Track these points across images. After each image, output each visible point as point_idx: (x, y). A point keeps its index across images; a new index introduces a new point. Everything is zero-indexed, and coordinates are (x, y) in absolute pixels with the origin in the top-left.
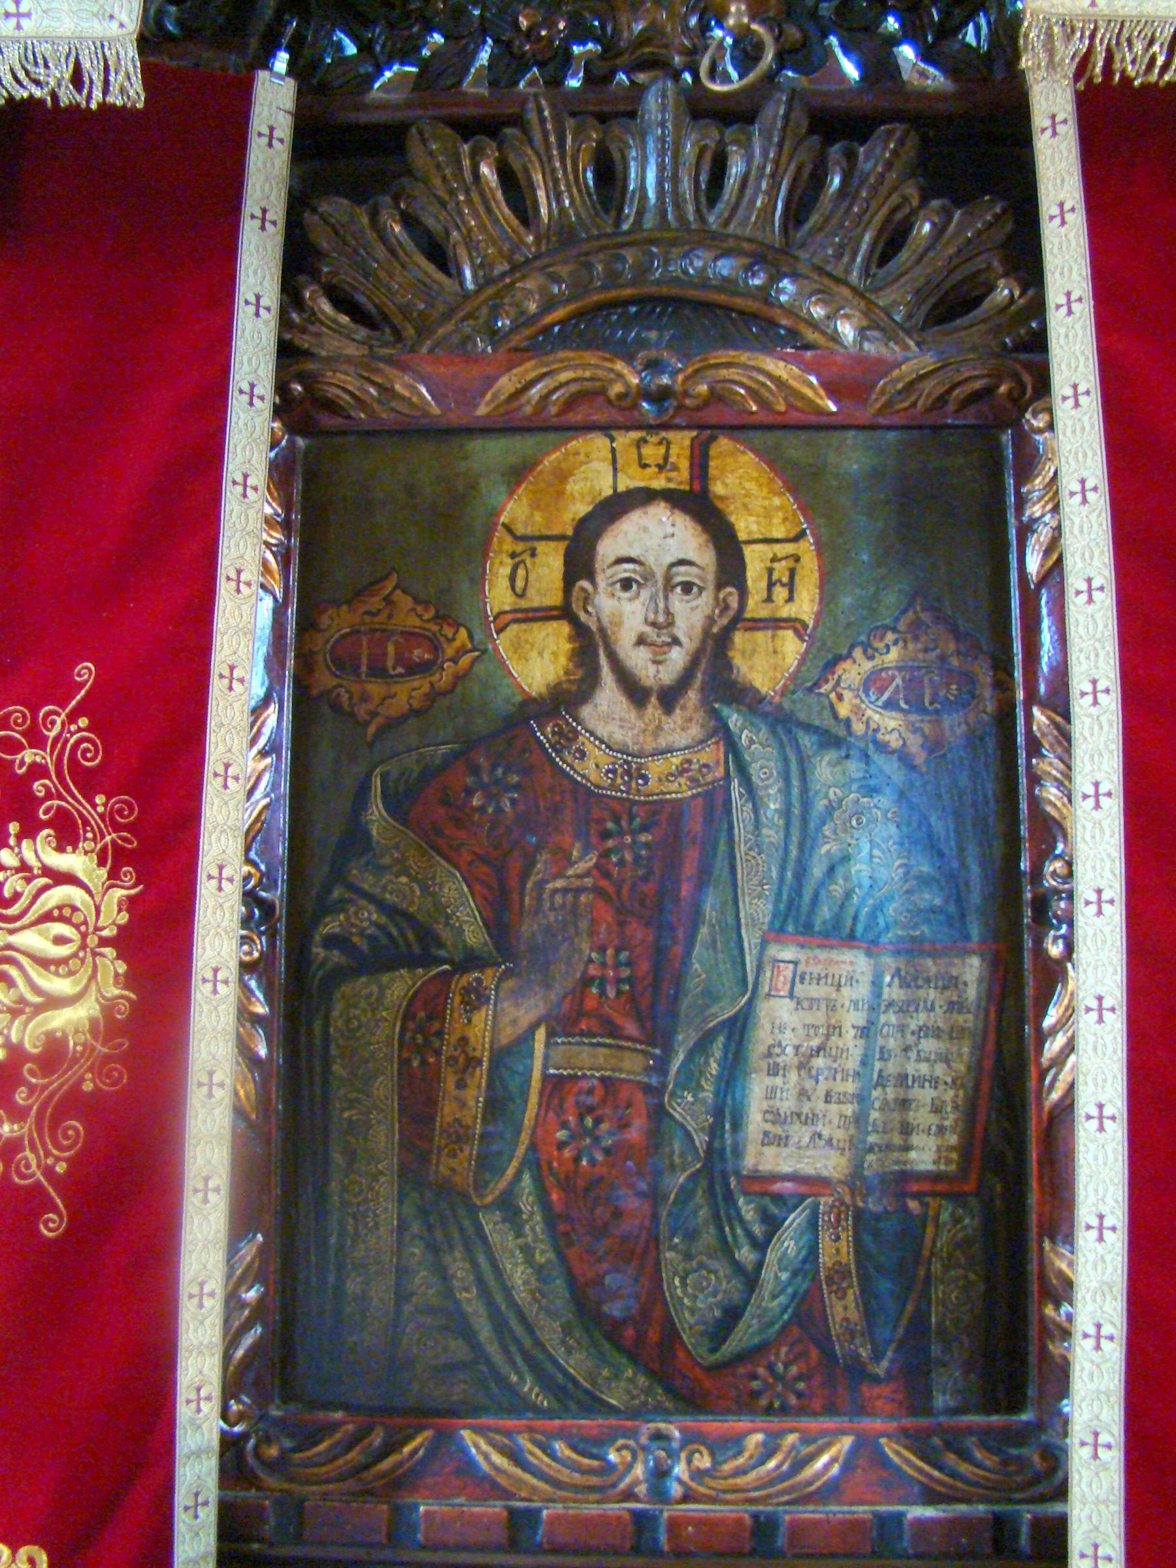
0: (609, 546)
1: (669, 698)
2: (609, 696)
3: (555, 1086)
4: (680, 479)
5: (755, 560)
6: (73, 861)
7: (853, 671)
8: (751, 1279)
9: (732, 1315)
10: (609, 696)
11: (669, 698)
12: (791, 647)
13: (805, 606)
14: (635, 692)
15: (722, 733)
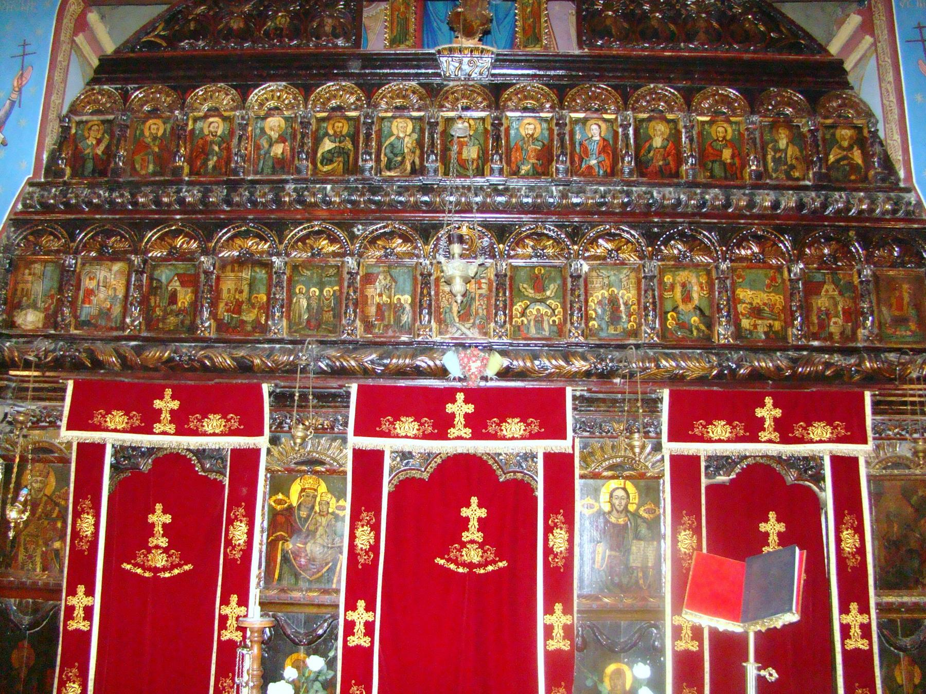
0: (614, 494)
1: (621, 512)
2: (615, 512)
3: (610, 556)
4: (622, 486)
5: (631, 496)
6: (563, 532)
7: (642, 509)
8: (631, 578)
9: (629, 582)
10: (615, 512)
11: (621, 512)
12: (635, 506)
13: (637, 501)
14: (618, 511)
15: (627, 516)
